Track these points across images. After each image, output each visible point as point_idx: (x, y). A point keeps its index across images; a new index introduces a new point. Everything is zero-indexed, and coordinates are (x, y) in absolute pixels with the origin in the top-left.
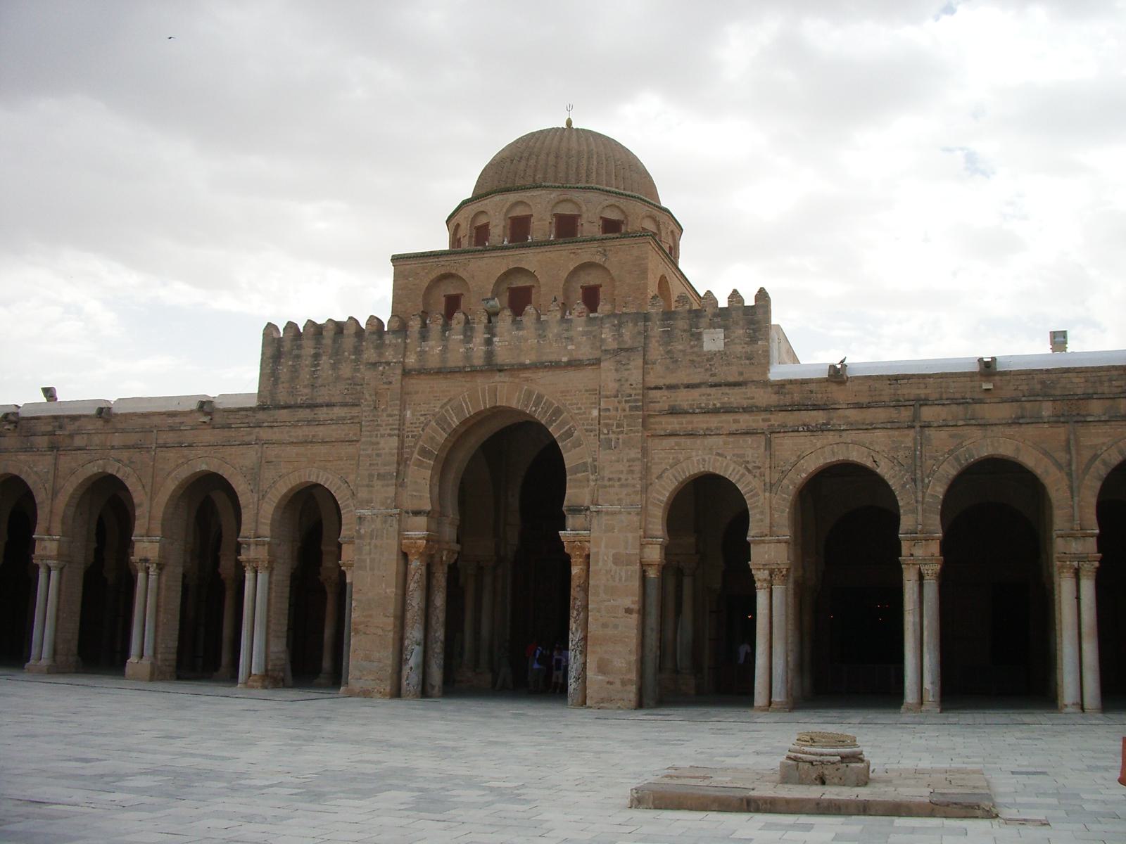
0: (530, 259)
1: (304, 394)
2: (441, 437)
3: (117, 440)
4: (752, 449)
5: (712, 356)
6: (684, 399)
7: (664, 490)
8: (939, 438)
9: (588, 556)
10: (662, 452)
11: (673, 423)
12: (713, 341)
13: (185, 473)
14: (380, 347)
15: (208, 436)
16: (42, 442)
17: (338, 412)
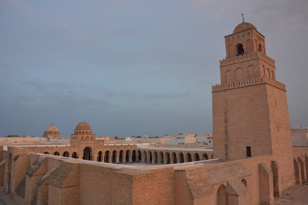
0: (88, 135)
1: (74, 145)
2: (84, 148)
3: (58, 149)
4: (103, 149)
5: (101, 144)
6: (99, 146)
7: (98, 152)
8: (112, 149)
9: (94, 157)
10: (98, 149)
11: (99, 148)
12: (101, 143)
13: (64, 151)
14: (80, 142)
15: (66, 148)
16: (50, 149)
17: (77, 147)
